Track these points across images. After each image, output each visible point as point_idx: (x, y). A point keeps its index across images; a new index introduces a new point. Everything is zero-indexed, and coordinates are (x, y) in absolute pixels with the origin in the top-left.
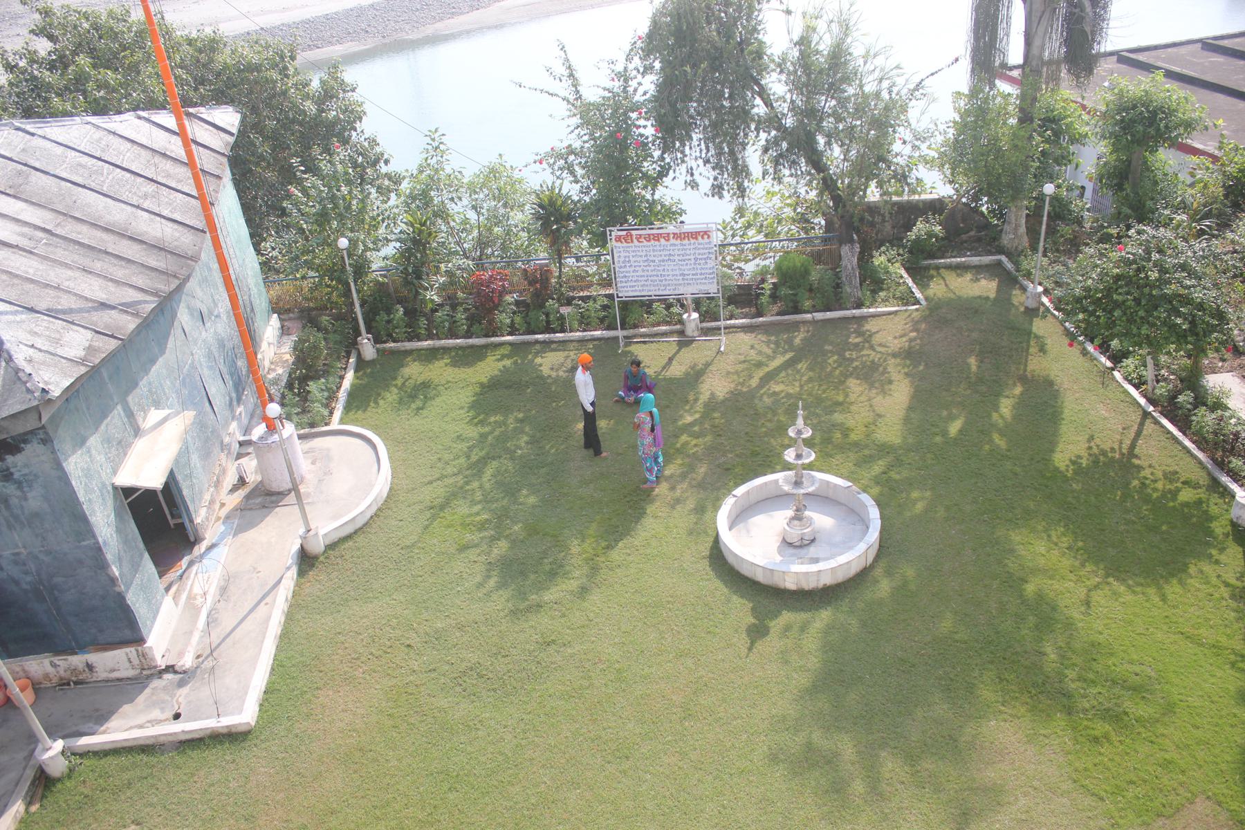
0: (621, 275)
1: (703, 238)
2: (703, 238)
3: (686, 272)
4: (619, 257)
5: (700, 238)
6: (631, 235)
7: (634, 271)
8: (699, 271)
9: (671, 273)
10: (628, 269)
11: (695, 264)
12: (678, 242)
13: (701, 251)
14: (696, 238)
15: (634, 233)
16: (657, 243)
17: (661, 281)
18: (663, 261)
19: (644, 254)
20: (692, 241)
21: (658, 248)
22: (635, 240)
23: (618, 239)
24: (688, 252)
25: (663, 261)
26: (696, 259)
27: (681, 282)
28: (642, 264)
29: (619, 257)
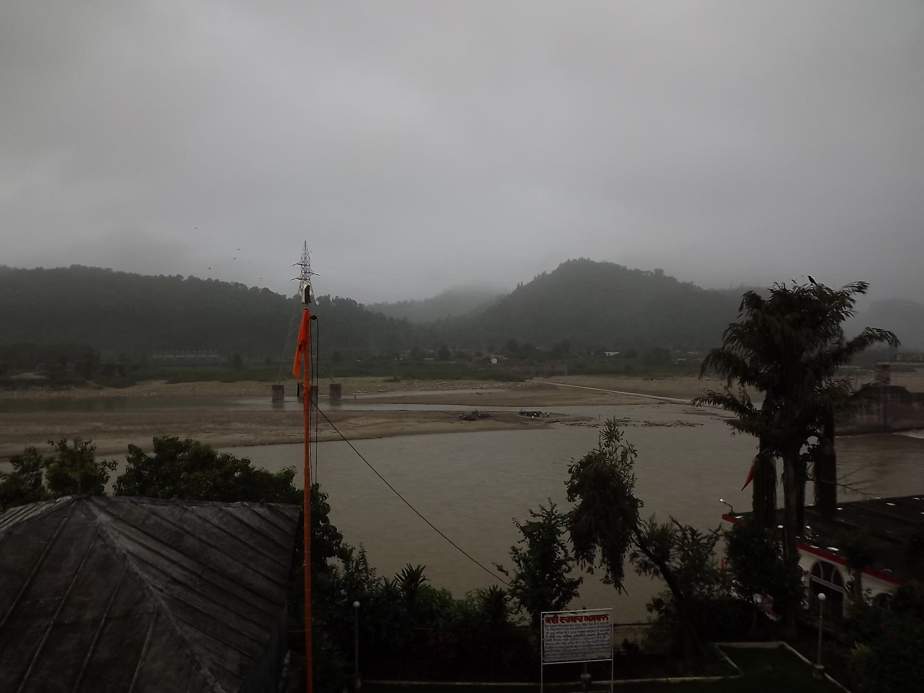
0: (548, 646)
1: (604, 619)
2: (604, 619)
3: (592, 644)
5: (602, 619)
6: (557, 617)
7: (557, 644)
8: (600, 643)
9: (581, 644)
10: (552, 642)
11: (598, 638)
12: (588, 622)
13: (601, 629)
14: (600, 620)
15: (559, 616)
16: (574, 623)
17: (574, 650)
18: (577, 636)
21: (575, 627)
22: (559, 622)
23: (548, 620)
26: (598, 634)
27: (588, 651)
28: (562, 638)
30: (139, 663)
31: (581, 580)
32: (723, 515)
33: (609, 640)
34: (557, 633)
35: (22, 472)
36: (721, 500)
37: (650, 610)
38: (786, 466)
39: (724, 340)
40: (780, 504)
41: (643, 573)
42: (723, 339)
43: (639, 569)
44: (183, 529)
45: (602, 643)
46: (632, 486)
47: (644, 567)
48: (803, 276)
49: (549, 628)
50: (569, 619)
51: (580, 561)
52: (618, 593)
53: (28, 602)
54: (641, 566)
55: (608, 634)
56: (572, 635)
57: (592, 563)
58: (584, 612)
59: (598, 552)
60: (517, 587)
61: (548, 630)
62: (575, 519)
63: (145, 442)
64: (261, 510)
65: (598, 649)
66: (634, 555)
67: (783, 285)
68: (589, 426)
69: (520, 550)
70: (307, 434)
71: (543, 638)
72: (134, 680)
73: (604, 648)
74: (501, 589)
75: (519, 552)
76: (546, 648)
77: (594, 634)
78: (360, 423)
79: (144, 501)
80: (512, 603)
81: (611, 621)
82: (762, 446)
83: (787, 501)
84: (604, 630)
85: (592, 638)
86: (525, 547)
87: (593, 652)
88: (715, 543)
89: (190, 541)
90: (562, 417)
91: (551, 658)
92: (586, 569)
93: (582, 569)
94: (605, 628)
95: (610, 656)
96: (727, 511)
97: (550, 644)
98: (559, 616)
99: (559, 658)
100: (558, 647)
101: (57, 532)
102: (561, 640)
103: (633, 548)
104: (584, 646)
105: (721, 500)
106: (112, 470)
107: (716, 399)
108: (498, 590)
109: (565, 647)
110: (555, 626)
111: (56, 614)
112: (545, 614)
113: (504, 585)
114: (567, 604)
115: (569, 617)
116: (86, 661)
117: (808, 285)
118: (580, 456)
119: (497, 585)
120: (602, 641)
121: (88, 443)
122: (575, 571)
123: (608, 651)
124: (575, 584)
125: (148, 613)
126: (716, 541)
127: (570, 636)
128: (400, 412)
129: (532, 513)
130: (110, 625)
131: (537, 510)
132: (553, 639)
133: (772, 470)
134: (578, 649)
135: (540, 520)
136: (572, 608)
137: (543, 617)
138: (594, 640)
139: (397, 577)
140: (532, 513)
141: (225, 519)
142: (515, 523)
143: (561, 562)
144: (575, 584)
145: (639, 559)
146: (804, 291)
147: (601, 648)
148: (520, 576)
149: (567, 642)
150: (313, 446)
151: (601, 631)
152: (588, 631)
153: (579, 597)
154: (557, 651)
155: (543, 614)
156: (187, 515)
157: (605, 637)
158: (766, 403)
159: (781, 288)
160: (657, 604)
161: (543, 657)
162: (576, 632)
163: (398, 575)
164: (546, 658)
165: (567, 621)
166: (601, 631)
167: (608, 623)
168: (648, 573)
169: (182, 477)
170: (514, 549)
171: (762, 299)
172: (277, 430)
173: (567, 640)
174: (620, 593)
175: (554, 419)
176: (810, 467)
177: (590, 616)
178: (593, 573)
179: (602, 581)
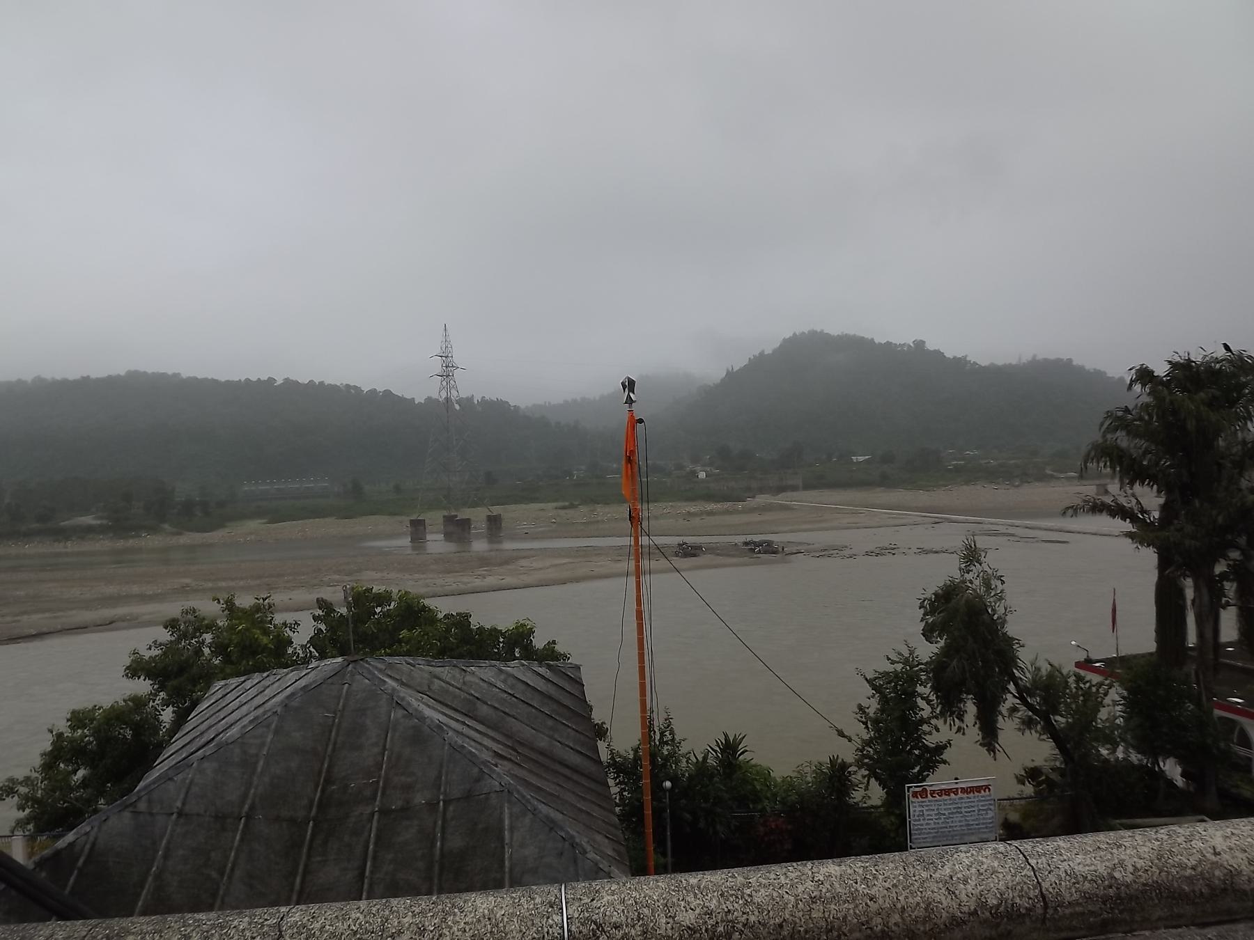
1: (985, 791)
2: (985, 791)
4: (915, 811)
5: (982, 791)
10: (922, 822)
12: (965, 795)
13: (982, 803)
14: (979, 792)
16: (947, 797)
17: (949, 832)
18: (952, 813)
19: (935, 808)
20: (976, 794)
23: (915, 795)
24: (972, 804)
25: (952, 813)
26: (979, 810)
27: (966, 832)
29: (915, 811)
30: (506, 850)
31: (949, 742)
32: (1076, 663)
33: (993, 817)
34: (927, 810)
35: (178, 640)
36: (1073, 643)
37: (1021, 781)
38: (1197, 588)
39: (1103, 430)
40: (1192, 639)
41: (1027, 732)
42: (1100, 429)
43: (1022, 727)
44: (472, 695)
45: (985, 821)
46: (1005, 622)
47: (1028, 724)
48: (1215, 342)
49: (917, 804)
50: (941, 793)
51: (948, 719)
52: (993, 759)
53: (335, 787)
54: (1023, 722)
55: (990, 809)
56: (946, 812)
57: (962, 721)
58: (957, 783)
59: (971, 708)
60: (864, 756)
61: (915, 807)
62: (938, 668)
63: (335, 595)
64: (542, 670)
65: (979, 829)
66: (1014, 710)
67: (1187, 355)
68: (843, 557)
69: (868, 708)
70: (637, 567)
71: (910, 817)
72: (507, 870)
73: (986, 828)
74: (843, 760)
75: (867, 710)
76: (914, 830)
77: (974, 811)
78: (535, 565)
79: (420, 662)
80: (859, 775)
81: (995, 793)
82: (1163, 565)
83: (1201, 635)
84: (986, 805)
85: (971, 816)
86: (873, 706)
87: (973, 834)
88: (1108, 691)
89: (484, 710)
90: (806, 547)
91: (920, 843)
92: (955, 729)
93: (951, 730)
94: (987, 803)
95: (994, 839)
96: (1081, 657)
97: (918, 825)
98: (929, 789)
99: (931, 842)
100: (929, 829)
101: (342, 701)
102: (932, 819)
103: (1010, 700)
104: (961, 826)
105: (1073, 643)
106: (294, 632)
107: (1097, 508)
108: (839, 761)
109: (938, 828)
110: (923, 802)
111: (378, 798)
112: (911, 787)
113: (848, 753)
114: (933, 774)
115: (941, 790)
116: (438, 852)
117: (1221, 353)
118: (934, 585)
119: (838, 756)
120: (984, 819)
121: (266, 599)
122: (939, 732)
123: (990, 832)
124: (940, 748)
125: (496, 791)
126: (1110, 688)
127: (944, 814)
128: (585, 548)
129: (889, 659)
130: (451, 808)
131: (894, 657)
132: (921, 818)
133: (1181, 593)
134: (954, 831)
135: (899, 667)
136: (937, 780)
137: (908, 791)
138: (975, 818)
139: (710, 750)
140: (889, 659)
141: (509, 683)
142: (860, 674)
143: (923, 721)
144: (940, 748)
145: (1020, 713)
146: (1217, 361)
147: (983, 828)
148: (868, 743)
149: (940, 821)
150: (645, 579)
151: (982, 806)
152: (965, 807)
153: (949, 764)
154: (927, 834)
155: (909, 787)
156: (468, 678)
157: (987, 813)
158: (1164, 508)
159: (1183, 358)
160: (1033, 774)
161: (910, 842)
162: (950, 808)
163: (710, 747)
164: (913, 843)
165: (939, 796)
166: (982, 806)
167: (990, 795)
168: (1033, 732)
169: (401, 636)
170: (861, 708)
171: (1155, 374)
172: (425, 579)
173: (940, 819)
174: (995, 760)
175: (794, 549)
176: (1230, 588)
177: (967, 788)
178: (964, 734)
179: (979, 743)
